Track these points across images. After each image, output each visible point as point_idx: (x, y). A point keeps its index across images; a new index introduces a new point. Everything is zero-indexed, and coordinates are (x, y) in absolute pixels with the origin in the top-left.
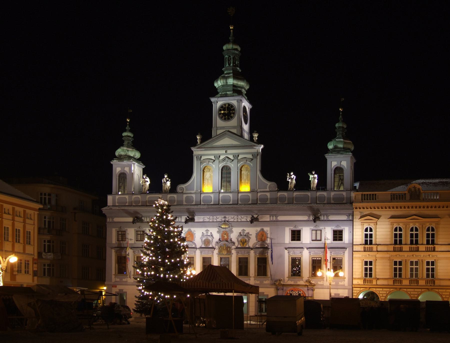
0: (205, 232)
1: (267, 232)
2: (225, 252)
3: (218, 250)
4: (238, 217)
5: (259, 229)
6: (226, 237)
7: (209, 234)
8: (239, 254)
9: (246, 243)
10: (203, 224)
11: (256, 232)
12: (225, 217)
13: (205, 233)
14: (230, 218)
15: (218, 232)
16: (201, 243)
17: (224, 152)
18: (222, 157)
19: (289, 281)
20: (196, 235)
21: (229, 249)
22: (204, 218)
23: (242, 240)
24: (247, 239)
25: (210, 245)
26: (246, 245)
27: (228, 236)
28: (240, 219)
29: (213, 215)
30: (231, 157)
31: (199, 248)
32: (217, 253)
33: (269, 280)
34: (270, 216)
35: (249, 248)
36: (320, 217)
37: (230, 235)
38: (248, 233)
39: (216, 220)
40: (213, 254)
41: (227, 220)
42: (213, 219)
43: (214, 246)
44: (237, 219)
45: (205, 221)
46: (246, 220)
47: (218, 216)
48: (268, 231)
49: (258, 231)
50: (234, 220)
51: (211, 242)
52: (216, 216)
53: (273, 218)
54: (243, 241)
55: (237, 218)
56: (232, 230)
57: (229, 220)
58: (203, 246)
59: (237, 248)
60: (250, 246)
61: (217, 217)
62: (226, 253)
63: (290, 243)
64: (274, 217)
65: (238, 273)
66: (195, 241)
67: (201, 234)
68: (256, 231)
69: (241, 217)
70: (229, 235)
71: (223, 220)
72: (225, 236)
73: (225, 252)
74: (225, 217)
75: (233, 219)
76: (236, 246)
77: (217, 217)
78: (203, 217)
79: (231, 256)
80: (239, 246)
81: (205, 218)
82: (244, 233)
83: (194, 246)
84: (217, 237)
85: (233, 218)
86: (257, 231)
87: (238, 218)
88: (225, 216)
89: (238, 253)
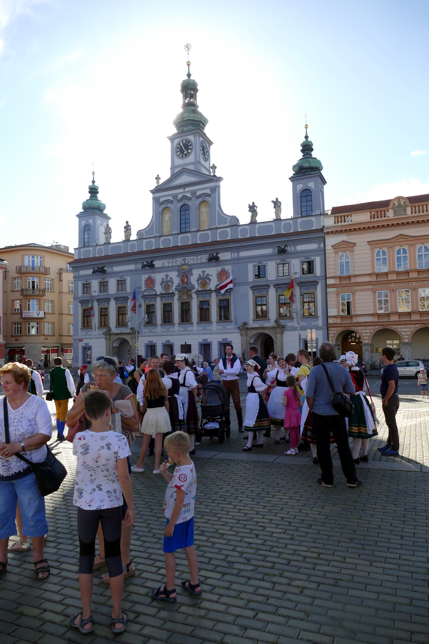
0: (165, 278)
2: (185, 297)
3: (178, 295)
5: (220, 268)
7: (169, 279)
10: (162, 269)
12: (184, 259)
14: (189, 259)
15: (178, 276)
17: (182, 190)
18: (180, 196)
24: (208, 281)
27: (188, 279)
29: (172, 259)
30: (189, 195)
35: (210, 290)
36: (286, 248)
38: (208, 274)
40: (173, 299)
42: (173, 262)
43: (174, 290)
44: (197, 259)
45: (165, 265)
47: (177, 259)
53: (234, 255)
58: (163, 292)
59: (198, 291)
62: (186, 298)
63: (254, 281)
64: (236, 254)
65: (199, 319)
66: (154, 287)
67: (161, 280)
71: (183, 262)
72: (185, 279)
74: (184, 259)
78: (162, 261)
79: (192, 301)
80: (200, 289)
81: (165, 262)
82: (204, 275)
83: (154, 293)
84: (177, 281)
89: (198, 297)
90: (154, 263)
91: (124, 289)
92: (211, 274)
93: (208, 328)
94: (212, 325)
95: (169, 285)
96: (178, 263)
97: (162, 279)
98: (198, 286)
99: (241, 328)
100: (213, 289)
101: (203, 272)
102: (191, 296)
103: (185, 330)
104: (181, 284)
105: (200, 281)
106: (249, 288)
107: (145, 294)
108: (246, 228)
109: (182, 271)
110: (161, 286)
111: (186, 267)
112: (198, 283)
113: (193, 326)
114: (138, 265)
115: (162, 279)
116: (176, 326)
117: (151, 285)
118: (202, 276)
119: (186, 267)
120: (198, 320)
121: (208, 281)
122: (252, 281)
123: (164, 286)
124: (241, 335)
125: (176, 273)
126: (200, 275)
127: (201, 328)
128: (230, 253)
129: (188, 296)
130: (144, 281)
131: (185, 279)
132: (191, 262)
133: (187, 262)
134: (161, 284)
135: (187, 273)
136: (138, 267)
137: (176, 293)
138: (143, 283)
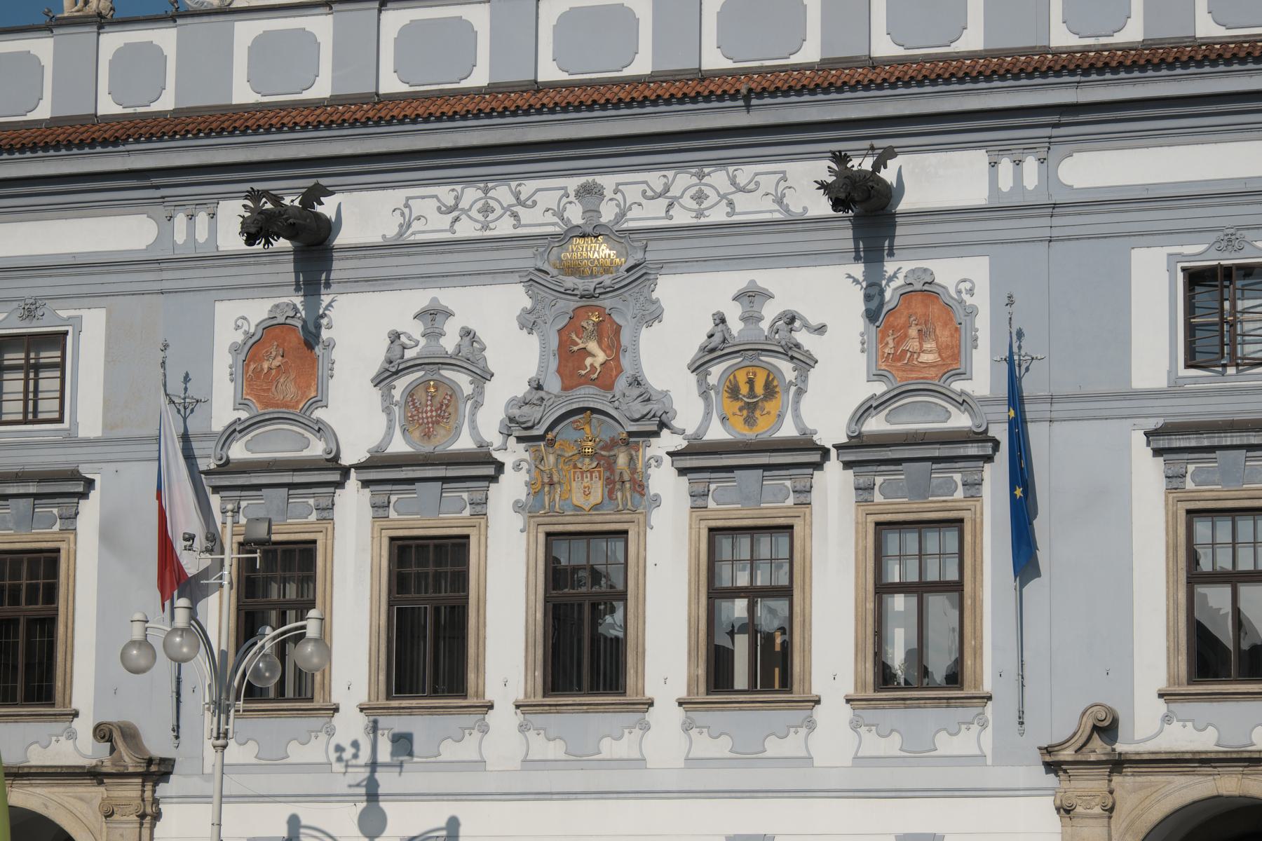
0: (415, 329)
3: (523, 476)
4: (706, 180)
6: (601, 357)
7: (450, 342)
8: (711, 504)
9: (770, 406)
13: (417, 336)
15: (529, 322)
16: (384, 417)
19: (1176, 725)
20: (336, 354)
21: (622, 460)
22: (407, 206)
23: (742, 378)
25: (457, 435)
26: (780, 417)
28: (723, 197)
31: (358, 467)
32: (523, 498)
33: (984, 726)
34: (993, 164)
35: (805, 444)
37: (635, 342)
38: (791, 319)
39: (512, 221)
41: (607, 213)
44: (700, 197)
45: (419, 232)
46: (780, 201)
47: (528, 187)
48: (971, 292)
50: (671, 205)
51: (469, 403)
52: (514, 184)
53: (1018, 177)
54: (751, 382)
55: (693, 191)
56: (654, 296)
57: (622, 215)
58: (399, 446)
59: (697, 448)
60: (810, 424)
61: (517, 196)
62: (597, 494)
63: (1175, 390)
65: (702, 671)
66: (320, 402)
69: (734, 183)
70: (625, 338)
71: (575, 215)
72: (592, 346)
73: (587, 494)
74: (589, 193)
75: (663, 202)
76: (690, 431)
77: (517, 196)
78: (397, 196)
79: (647, 524)
80: (717, 432)
81: (418, 207)
83: (317, 449)
85: (659, 189)
87: (707, 190)
88: (590, 178)
89: (698, 497)
90: (327, 207)
91: (48, 407)
92: (814, 321)
93: (774, 747)
94: (811, 725)
95: (453, 391)
96: (537, 220)
97: (395, 337)
98: (700, 404)
99: (1067, 754)
100: (831, 432)
101: (751, 297)
102: (640, 487)
103: (578, 759)
104: (553, 384)
105: (716, 372)
106: (1139, 438)
107: (238, 451)
109: (570, 282)
110: (376, 394)
111: (602, 251)
112: (702, 381)
113: (646, 727)
114: (180, 219)
115: (395, 337)
116: (504, 718)
117: (287, 389)
118: (735, 326)
119: (602, 251)
120: (692, 683)
121: (786, 368)
122: (1161, 382)
123: (411, 394)
124: (1065, 811)
125: (516, 297)
126: (721, 320)
127: (720, 748)
128: (979, 158)
129: (612, 484)
130: (235, 349)
131: (592, 346)
132: (649, 214)
133: (607, 213)
134: (384, 378)
135: (607, 302)
136: (180, 237)
137: (512, 454)
138: (223, 364)
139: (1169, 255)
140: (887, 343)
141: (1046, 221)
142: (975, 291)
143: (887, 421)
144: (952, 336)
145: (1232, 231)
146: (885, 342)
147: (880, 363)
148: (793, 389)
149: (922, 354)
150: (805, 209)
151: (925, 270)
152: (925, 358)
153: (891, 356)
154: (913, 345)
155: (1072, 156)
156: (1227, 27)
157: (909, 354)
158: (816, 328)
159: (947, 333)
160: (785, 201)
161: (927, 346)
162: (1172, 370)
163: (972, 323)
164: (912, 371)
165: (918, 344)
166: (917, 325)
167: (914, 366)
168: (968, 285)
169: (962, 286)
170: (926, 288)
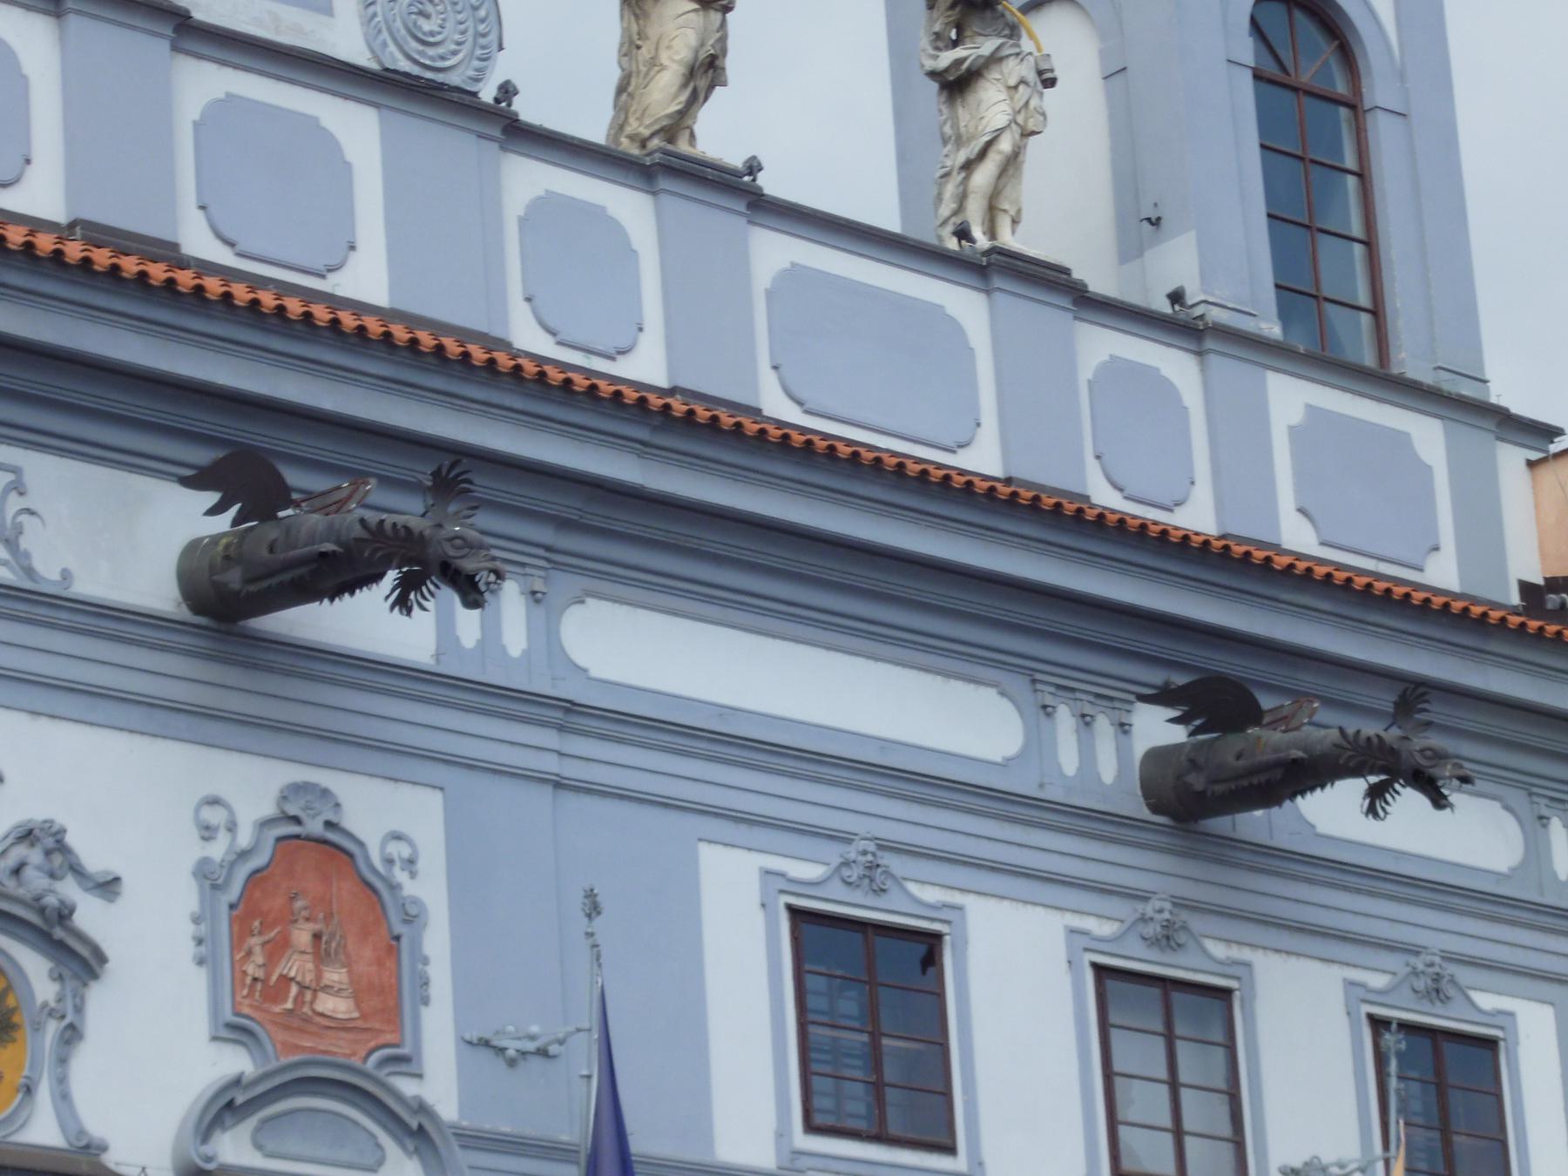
1: (410, 888)
11: (194, 833)
48: (410, 862)
49: (232, 827)
60: (96, 1125)
68: (208, 832)
86: (215, 816)
92: (95, 860)
108: (596, 214)
139: (768, 873)
140: (249, 953)
141: (549, 738)
142: (421, 865)
143: (258, 1146)
144: (380, 963)
145: (871, 847)
146: (246, 947)
147: (238, 999)
148: (52, 1028)
149: (321, 995)
150: (66, 575)
151: (325, 793)
152: (329, 1004)
153: (259, 986)
154: (297, 966)
155: (583, 602)
156: (806, 407)
157: (294, 990)
158: (101, 880)
159: (368, 953)
160: (24, 543)
161: (335, 975)
162: (782, 1134)
163: (416, 944)
164: (302, 1031)
165: (310, 966)
166: (308, 919)
167: (307, 1020)
168: (404, 850)
169: (396, 849)
170: (332, 836)
